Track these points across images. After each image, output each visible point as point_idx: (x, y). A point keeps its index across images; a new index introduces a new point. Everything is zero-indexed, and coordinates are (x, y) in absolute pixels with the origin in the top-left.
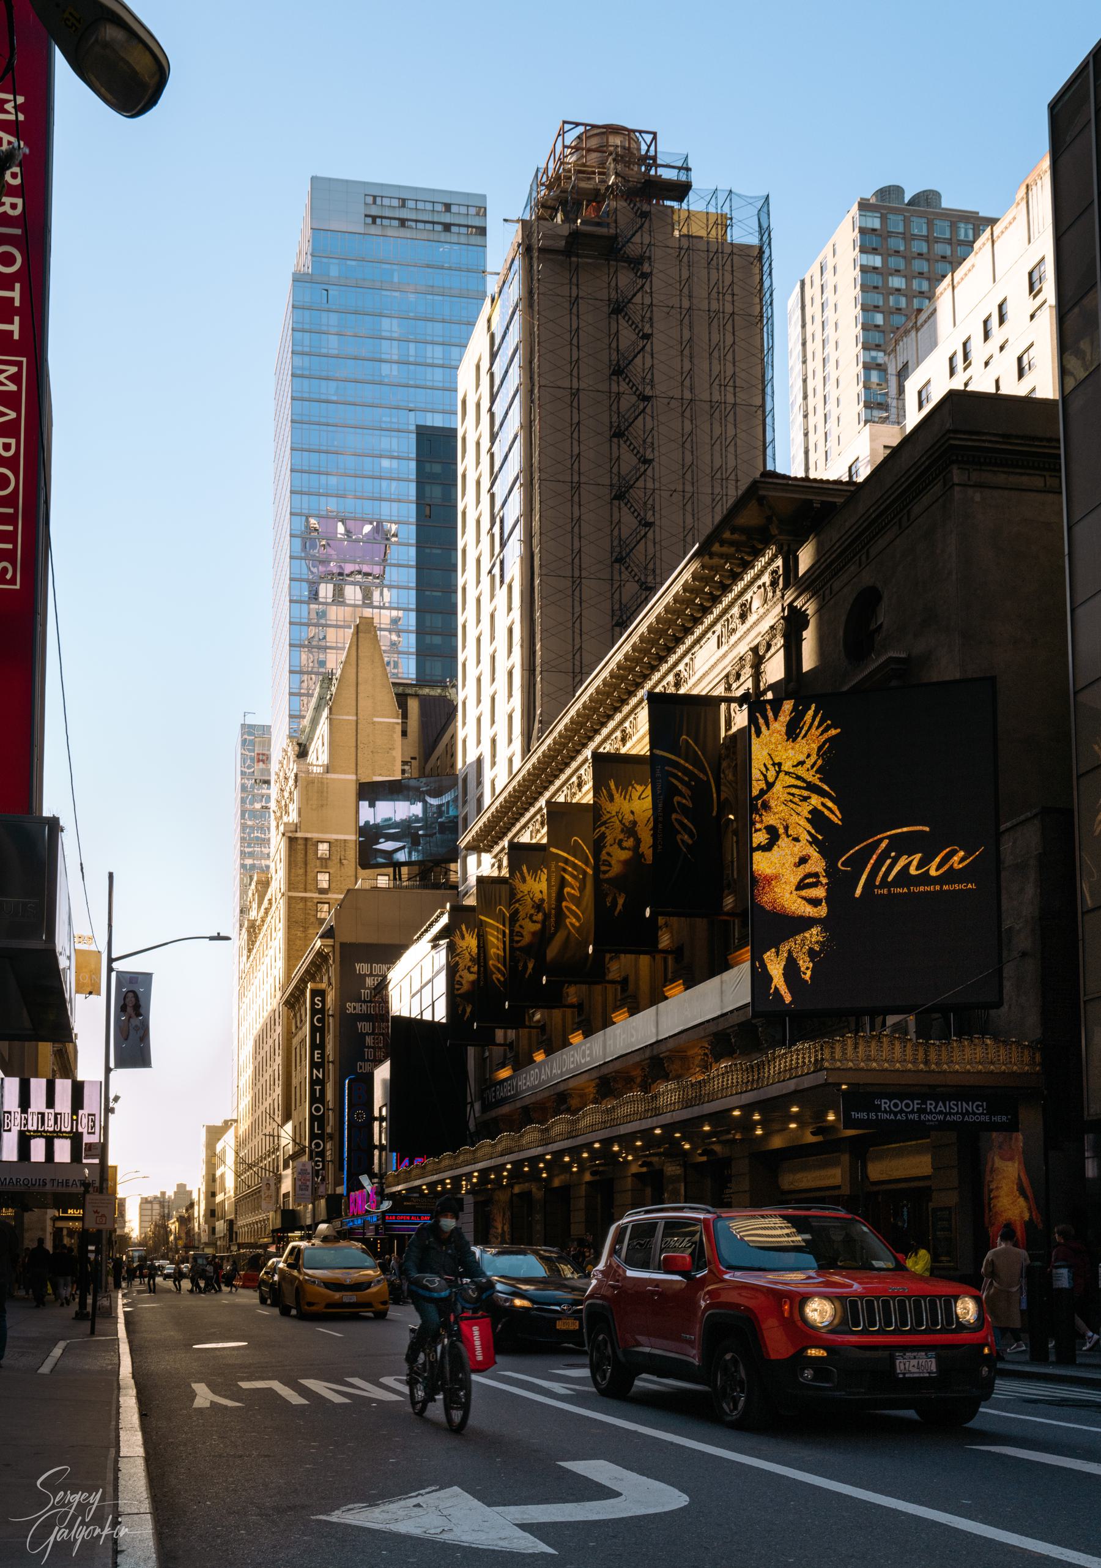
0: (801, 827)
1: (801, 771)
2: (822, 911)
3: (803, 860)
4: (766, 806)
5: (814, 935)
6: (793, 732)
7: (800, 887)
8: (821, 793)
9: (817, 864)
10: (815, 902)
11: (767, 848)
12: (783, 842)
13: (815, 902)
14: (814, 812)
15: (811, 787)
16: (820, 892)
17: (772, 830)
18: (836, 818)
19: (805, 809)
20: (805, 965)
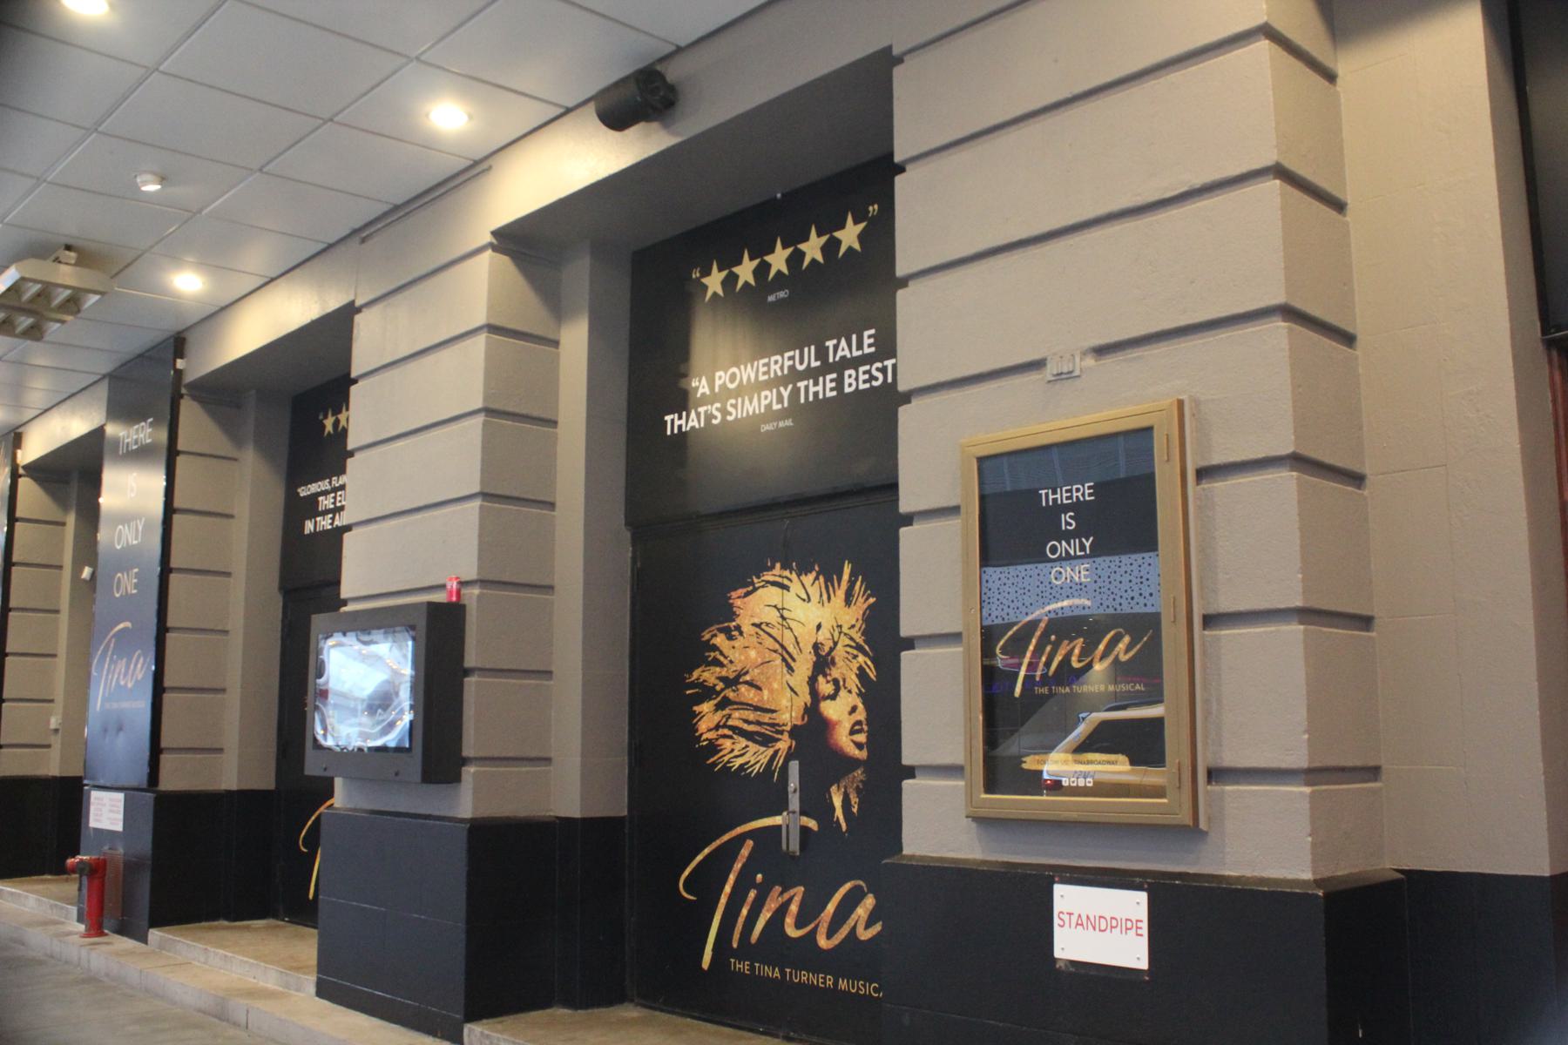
0: (853, 681)
1: (853, 633)
2: (862, 755)
3: (854, 709)
4: (833, 663)
5: (859, 773)
6: (848, 599)
7: (852, 732)
8: (865, 653)
9: (861, 715)
10: (859, 746)
11: (833, 697)
12: (843, 693)
13: (859, 746)
14: (860, 668)
15: (859, 648)
16: (861, 738)
17: (836, 682)
18: (872, 675)
19: (855, 665)
20: (854, 800)
